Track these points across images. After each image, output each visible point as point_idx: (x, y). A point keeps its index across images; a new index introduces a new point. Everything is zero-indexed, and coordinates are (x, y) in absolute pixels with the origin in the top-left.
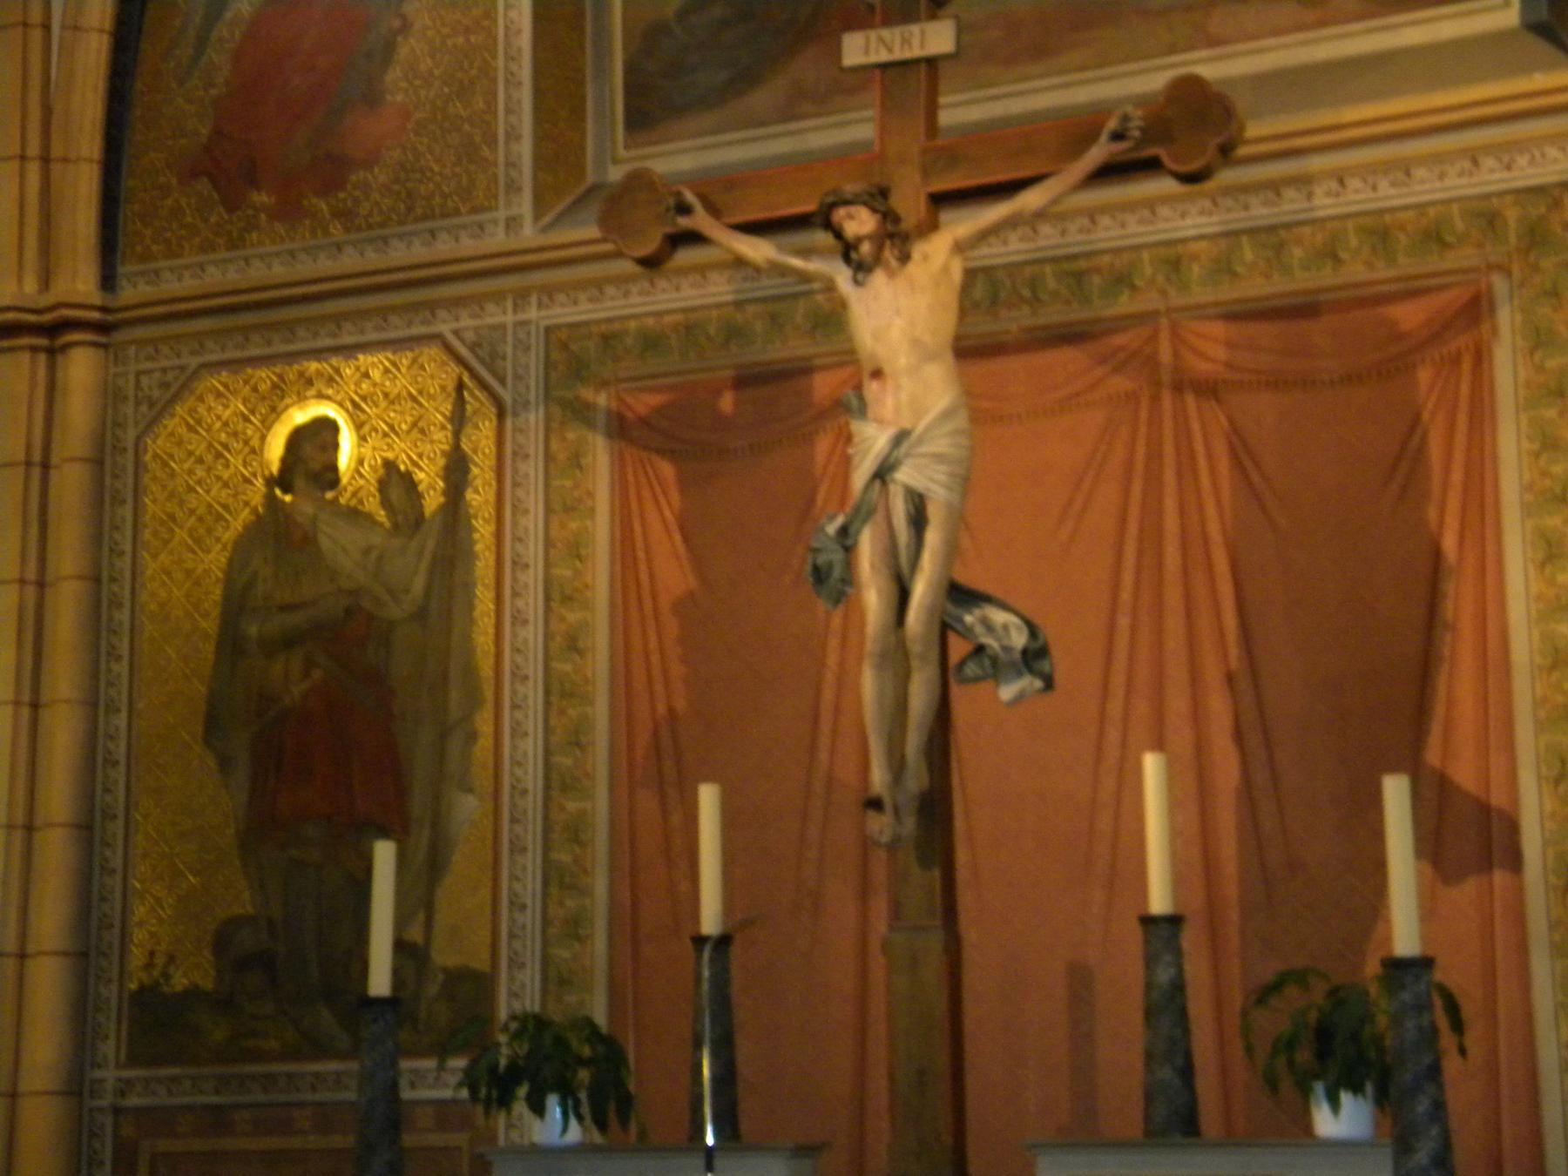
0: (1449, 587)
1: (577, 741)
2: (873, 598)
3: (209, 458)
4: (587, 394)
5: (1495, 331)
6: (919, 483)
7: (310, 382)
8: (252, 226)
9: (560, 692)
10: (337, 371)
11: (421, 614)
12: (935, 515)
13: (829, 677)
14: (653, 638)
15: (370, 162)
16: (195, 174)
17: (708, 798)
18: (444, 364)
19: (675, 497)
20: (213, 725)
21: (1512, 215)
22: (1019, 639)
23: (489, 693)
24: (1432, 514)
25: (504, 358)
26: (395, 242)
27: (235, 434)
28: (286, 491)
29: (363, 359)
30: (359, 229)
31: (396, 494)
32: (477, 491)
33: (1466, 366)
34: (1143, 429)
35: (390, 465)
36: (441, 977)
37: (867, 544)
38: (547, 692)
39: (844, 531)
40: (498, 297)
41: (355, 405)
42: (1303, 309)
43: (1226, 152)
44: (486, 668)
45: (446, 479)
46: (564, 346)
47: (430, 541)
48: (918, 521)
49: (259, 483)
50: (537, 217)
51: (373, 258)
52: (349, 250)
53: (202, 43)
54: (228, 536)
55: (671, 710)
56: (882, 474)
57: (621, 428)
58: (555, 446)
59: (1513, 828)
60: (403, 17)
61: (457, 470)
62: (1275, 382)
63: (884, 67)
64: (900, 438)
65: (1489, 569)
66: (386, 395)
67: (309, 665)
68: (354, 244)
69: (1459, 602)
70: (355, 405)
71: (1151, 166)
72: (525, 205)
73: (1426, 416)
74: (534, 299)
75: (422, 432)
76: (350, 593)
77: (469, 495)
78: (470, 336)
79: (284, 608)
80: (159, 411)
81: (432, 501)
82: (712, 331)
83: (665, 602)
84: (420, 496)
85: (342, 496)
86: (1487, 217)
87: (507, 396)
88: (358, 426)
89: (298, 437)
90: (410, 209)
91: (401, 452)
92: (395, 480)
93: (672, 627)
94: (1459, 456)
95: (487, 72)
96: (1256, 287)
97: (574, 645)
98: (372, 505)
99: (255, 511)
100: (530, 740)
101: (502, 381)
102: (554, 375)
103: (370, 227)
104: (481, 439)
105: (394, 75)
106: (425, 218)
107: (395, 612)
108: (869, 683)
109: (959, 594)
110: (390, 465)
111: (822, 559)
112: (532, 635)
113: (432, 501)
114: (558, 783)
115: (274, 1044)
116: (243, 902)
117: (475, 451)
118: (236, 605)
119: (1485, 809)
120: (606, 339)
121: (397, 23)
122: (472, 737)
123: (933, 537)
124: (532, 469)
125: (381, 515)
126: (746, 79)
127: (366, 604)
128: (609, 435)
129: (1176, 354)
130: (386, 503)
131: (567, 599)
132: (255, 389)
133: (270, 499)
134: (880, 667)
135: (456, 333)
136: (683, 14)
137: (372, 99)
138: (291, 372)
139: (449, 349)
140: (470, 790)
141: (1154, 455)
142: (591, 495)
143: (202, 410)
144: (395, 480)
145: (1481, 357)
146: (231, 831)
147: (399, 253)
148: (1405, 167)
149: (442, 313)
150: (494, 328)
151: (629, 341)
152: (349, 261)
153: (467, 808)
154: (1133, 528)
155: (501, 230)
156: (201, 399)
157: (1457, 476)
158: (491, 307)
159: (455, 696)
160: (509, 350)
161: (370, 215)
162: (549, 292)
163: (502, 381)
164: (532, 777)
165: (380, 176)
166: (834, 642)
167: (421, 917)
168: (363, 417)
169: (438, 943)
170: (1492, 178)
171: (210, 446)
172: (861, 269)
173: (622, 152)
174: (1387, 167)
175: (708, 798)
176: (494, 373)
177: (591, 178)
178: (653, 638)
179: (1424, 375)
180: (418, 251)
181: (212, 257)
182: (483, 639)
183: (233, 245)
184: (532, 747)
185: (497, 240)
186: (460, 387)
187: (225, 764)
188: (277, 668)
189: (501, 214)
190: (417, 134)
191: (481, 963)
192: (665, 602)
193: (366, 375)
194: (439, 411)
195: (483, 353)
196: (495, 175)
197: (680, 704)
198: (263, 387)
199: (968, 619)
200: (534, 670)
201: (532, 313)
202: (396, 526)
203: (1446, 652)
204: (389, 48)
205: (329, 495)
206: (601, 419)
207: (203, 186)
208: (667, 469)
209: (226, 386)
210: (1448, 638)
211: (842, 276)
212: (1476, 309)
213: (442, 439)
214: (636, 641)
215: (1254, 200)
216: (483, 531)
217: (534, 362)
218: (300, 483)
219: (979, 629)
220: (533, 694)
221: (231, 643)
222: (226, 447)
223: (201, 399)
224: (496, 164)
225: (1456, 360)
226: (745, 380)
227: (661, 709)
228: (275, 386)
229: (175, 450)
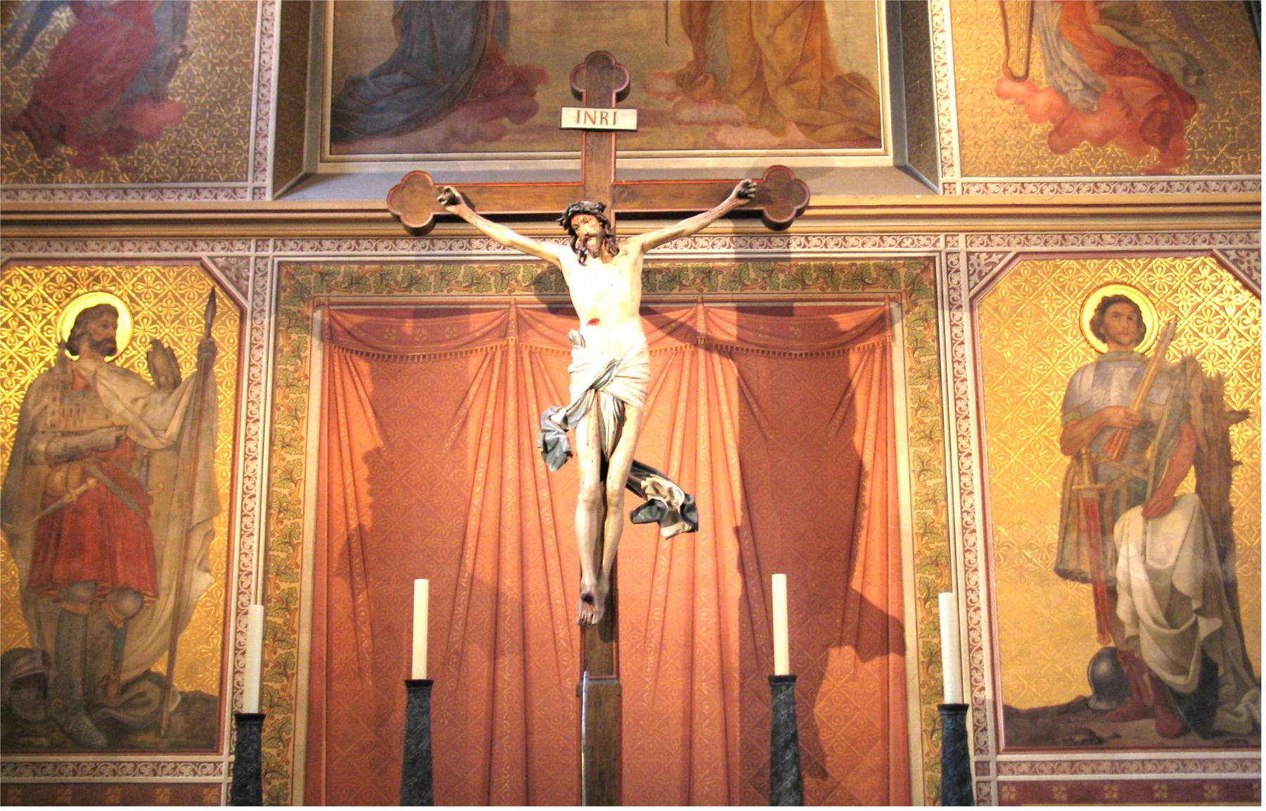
0: (867, 484)
1: (291, 540)
3: (13, 324)
4: (308, 311)
5: (893, 336)
6: (623, 396)
7: (97, 280)
8: (56, 169)
9: (277, 509)
10: (119, 274)
11: (175, 447)
12: (631, 414)
13: (474, 511)
14: (348, 474)
15: (152, 139)
16: (15, 128)
17: (421, 588)
18: (201, 279)
19: (368, 382)
21: (902, 271)
22: (679, 499)
23: (225, 507)
24: (857, 439)
25: (247, 279)
26: (169, 193)
27: (36, 309)
28: (73, 353)
29: (142, 270)
30: (142, 181)
31: (160, 361)
32: (222, 367)
33: (878, 354)
34: (686, 372)
35: (156, 343)
36: (179, 698)
38: (269, 507)
39: (565, 420)
40: (245, 238)
41: (132, 300)
42: (785, 311)
43: (799, 213)
44: (224, 489)
45: (199, 356)
46: (292, 277)
47: (184, 397)
48: (621, 420)
49: (53, 345)
50: (275, 190)
51: (150, 202)
52: (133, 194)
53: (28, 41)
54: (28, 379)
55: (360, 526)
56: (595, 387)
57: (330, 336)
58: (281, 342)
59: (901, 628)
60: (184, 47)
61: (207, 352)
62: (768, 352)
63: (587, 131)
64: (611, 366)
65: (889, 474)
66: (156, 295)
67: (85, 476)
68: (138, 190)
69: (872, 491)
70: (132, 300)
71: (758, 215)
72: (268, 181)
73: (855, 382)
74: (271, 243)
75: (182, 322)
76: (121, 427)
77: (216, 368)
78: (221, 262)
79: (66, 434)
81: (188, 369)
82: (399, 278)
83: (359, 453)
84: (178, 366)
85: (1190, 397)
87: (248, 305)
88: (134, 315)
90: (180, 174)
91: (167, 334)
92: (161, 355)
93: (363, 471)
94: (873, 407)
95: (246, 92)
96: (756, 294)
97: (290, 476)
98: (142, 369)
99: (48, 364)
100: (255, 538)
101: (245, 295)
102: (283, 295)
103: (150, 181)
104: (224, 333)
105: (173, 84)
106: (192, 180)
107: (152, 442)
108: (582, 521)
109: (638, 469)
110: (156, 343)
111: (549, 437)
112: (259, 467)
113: (188, 369)
114: (274, 570)
115: (44, 741)
117: (223, 339)
118: (26, 430)
119: (885, 617)
120: (322, 275)
121: (179, 51)
122: (210, 534)
123: (629, 429)
124: (264, 357)
125: (148, 377)
126: (417, 122)
127: (133, 436)
128: (322, 339)
129: (708, 329)
130: (152, 368)
131: (286, 445)
132: (53, 280)
133: (61, 360)
134: (590, 510)
135: (211, 258)
136: (376, 75)
137: (157, 97)
138: (83, 271)
139: (204, 266)
140: (207, 571)
141: (503, 380)
142: (307, 377)
143: (10, 290)
144: (161, 355)
145: (886, 351)
146: (16, 589)
147: (171, 201)
148: (844, 235)
149: (202, 245)
150: (241, 258)
151: (340, 278)
152: (133, 201)
153: (203, 584)
154: (678, 433)
155: (249, 194)
156: (9, 282)
157: (872, 418)
158: (238, 245)
159: (198, 505)
160: (251, 274)
161: (151, 172)
162: (283, 239)
163: (245, 295)
164: (255, 564)
165: (160, 148)
166: (478, 489)
167: (166, 654)
168: (138, 308)
169: (178, 672)
170: (889, 249)
171: (15, 316)
173: (328, 156)
174: (834, 234)
175: (421, 588)
176: (239, 289)
177: (305, 170)
178: (348, 474)
179: (854, 358)
180: (186, 202)
181: (25, 185)
182: (222, 469)
183: (42, 180)
184: (256, 543)
185: (245, 200)
186: (213, 295)
187: (12, 540)
188: (58, 477)
189: (250, 184)
190: (189, 124)
191: (212, 689)
192: (359, 453)
193: (141, 280)
194: (195, 310)
195: (232, 274)
196: (247, 159)
197: (367, 521)
198: (60, 279)
199: (643, 484)
200: (260, 490)
201: (269, 252)
202: (159, 386)
203: (865, 522)
204: (172, 67)
205: (108, 359)
206: (317, 329)
207: (21, 137)
208: (364, 367)
209: (31, 276)
210: (866, 514)
212: (882, 323)
213: (198, 330)
214: (337, 479)
215: (756, 243)
216: (225, 396)
217: (269, 284)
218: (85, 347)
219: (649, 491)
220: (258, 506)
222: (28, 317)
223: (9, 282)
224: (248, 151)
225: (872, 351)
226: (421, 313)
227: (353, 524)
228: (69, 279)
229: (32, 314)
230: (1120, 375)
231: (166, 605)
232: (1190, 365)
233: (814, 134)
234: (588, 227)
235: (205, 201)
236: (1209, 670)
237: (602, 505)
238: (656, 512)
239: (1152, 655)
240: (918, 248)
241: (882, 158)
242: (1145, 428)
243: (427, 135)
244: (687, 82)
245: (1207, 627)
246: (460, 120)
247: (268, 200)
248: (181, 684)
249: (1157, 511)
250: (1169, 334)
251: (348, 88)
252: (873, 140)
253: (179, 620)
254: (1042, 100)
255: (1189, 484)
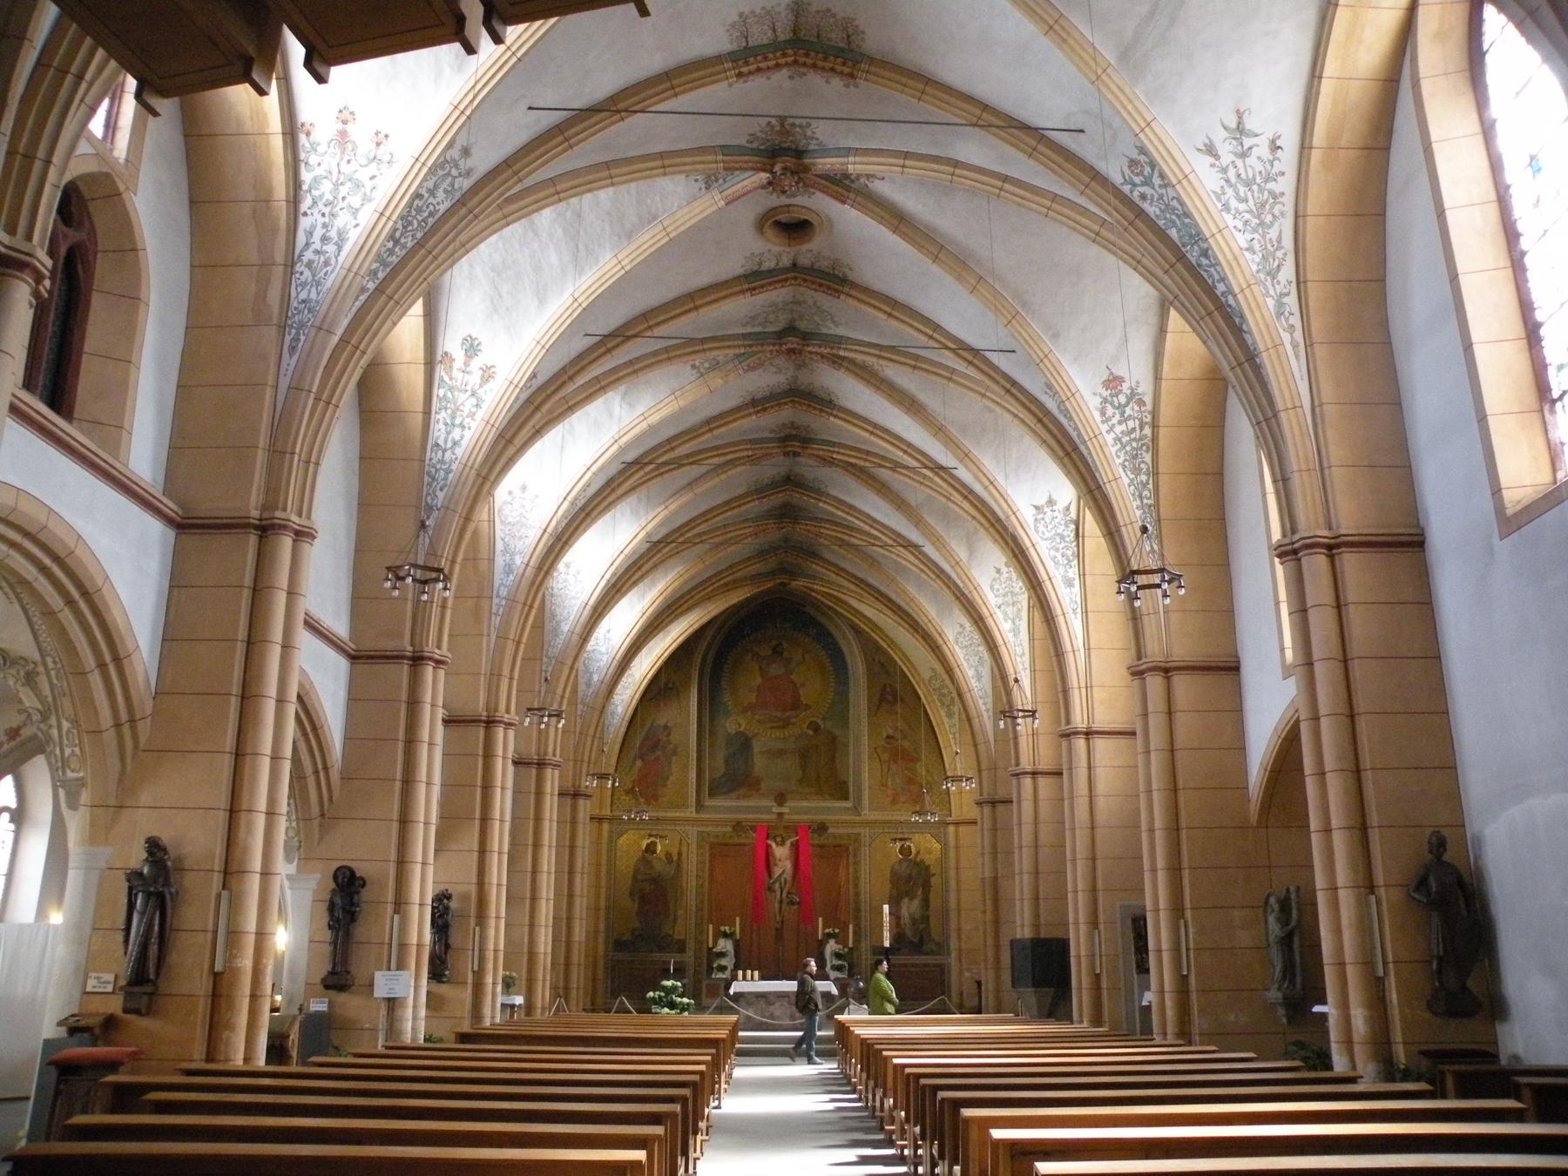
2: (778, 893)
17: (738, 919)
20: (631, 894)
37: (777, 885)
61: (680, 854)
80: (621, 835)
81: (675, 859)
86: (849, 835)
89: (648, 845)
92: (668, 855)
104: (684, 849)
108: (777, 905)
109: (789, 893)
113: (675, 859)
116: (637, 925)
118: (636, 871)
126: (731, 790)
137: (665, 786)
144: (668, 855)
153: (680, 912)
164: (694, 908)
172: (777, 844)
175: (738, 919)
184: (693, 903)
185: (688, 814)
211: (774, 845)
216: (685, 866)
221: (635, 879)
230: (905, 864)
231: (672, 917)
232: (922, 861)
233: (833, 797)
234: (779, 839)
235: (677, 814)
236: (921, 939)
237: (781, 902)
238: (792, 903)
239: (909, 933)
240: (856, 831)
241: (848, 804)
242: (910, 877)
243: (734, 795)
244: (800, 781)
245: (922, 926)
246: (741, 791)
247: (694, 814)
248: (676, 937)
249: (911, 899)
250: (918, 853)
251: (712, 781)
252: (847, 798)
253: (675, 920)
254: (889, 792)
255: (919, 892)
